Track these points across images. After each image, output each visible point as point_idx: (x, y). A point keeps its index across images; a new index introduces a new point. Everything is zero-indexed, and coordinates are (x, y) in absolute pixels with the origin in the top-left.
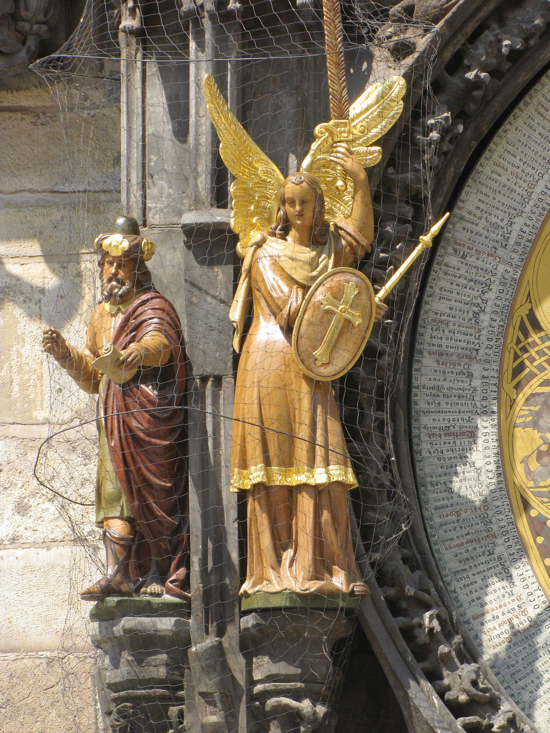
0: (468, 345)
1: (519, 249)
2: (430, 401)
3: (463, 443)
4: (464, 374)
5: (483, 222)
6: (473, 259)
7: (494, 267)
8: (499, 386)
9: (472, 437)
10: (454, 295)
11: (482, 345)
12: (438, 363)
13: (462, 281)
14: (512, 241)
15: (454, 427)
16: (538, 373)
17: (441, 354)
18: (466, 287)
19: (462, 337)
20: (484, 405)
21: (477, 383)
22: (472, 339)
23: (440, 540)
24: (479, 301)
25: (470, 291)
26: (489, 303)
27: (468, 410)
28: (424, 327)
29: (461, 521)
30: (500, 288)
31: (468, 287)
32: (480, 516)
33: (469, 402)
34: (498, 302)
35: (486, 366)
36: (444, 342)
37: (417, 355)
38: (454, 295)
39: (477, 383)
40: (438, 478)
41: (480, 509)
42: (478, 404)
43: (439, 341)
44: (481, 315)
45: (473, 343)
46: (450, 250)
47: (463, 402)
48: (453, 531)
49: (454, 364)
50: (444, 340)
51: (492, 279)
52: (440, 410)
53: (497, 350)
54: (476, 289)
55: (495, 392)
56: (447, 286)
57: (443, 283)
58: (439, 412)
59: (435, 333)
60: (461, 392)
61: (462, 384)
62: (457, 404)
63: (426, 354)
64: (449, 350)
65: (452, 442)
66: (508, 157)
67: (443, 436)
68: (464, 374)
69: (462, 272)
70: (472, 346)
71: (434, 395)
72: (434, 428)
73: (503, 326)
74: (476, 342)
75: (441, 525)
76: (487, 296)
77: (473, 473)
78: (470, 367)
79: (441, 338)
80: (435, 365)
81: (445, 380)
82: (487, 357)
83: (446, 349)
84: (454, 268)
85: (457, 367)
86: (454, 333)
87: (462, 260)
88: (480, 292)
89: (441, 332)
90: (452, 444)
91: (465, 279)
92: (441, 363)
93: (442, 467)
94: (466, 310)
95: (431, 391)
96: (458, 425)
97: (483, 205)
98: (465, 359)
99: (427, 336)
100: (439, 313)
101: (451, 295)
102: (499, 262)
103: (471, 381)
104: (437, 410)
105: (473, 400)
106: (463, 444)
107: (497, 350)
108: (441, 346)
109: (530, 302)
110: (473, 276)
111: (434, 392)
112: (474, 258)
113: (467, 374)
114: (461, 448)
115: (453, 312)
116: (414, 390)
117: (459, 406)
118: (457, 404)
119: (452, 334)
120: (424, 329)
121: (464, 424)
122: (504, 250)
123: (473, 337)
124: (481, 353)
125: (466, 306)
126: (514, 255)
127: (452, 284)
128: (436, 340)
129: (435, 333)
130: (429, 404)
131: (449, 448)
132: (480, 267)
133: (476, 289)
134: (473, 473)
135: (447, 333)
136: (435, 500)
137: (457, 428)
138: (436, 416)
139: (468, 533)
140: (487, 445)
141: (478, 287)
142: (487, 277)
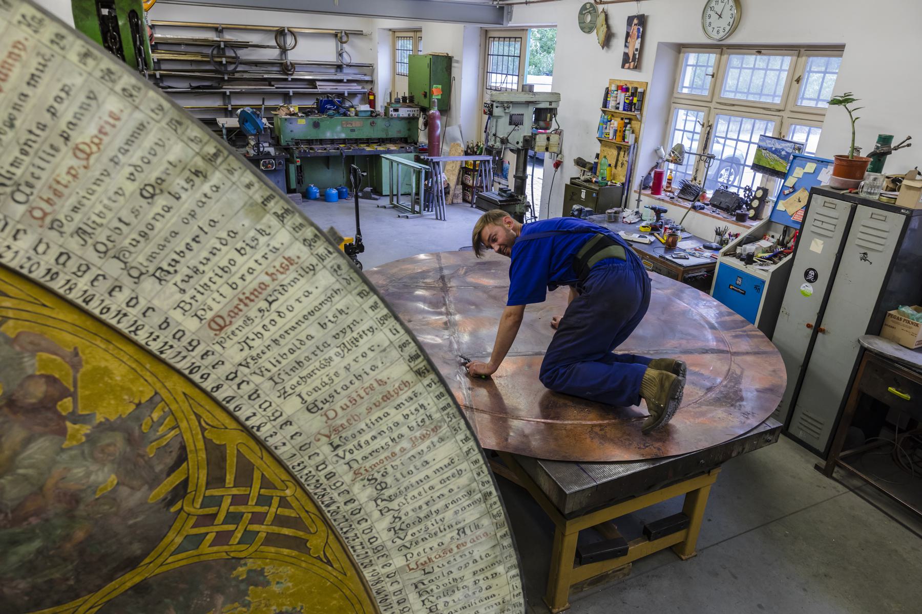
0: (356, 443)
1: (394, 598)
2: (342, 317)
3: (219, 298)
4: (325, 402)
5: (469, 581)
6: (446, 540)
7: (409, 556)
9: (213, 320)
10: (435, 482)
11: (335, 459)
12: (381, 383)
13: (440, 505)
15: (260, 310)
16: (208, 493)
17: (387, 397)
18: (427, 504)
19: (375, 445)
20: (244, 386)
22: (358, 455)
23: (58, 59)
24: (394, 505)
25: (417, 505)
26: (376, 514)
27: (264, 357)
28: (444, 409)
29: (59, 142)
30: (379, 541)
31: (424, 507)
32: (29, 185)
33: (274, 370)
34: (364, 525)
35: (299, 440)
36: (396, 416)
37: (421, 365)
38: (435, 482)
39: (291, 406)
40: (198, 195)
41: (48, 201)
42: (257, 379)
43: (406, 412)
44: (375, 492)
45: (351, 452)
47: (284, 362)
48: (51, 101)
49: (353, 401)
50: (400, 418)
51: (399, 542)
52: (312, 318)
53: (306, 471)
54: (411, 513)
55: (247, 419)
56: (454, 484)
58: (311, 313)
59: (422, 414)
60: (304, 373)
61: (314, 385)
62: (292, 351)
63: (410, 377)
64: (380, 414)
65: (240, 282)
67: (266, 279)
68: (325, 402)
69: (449, 515)
70: (350, 446)
71: (343, 332)
72: (295, 280)
73: (328, 506)
74: (348, 457)
75: (92, 96)
76: (388, 518)
77: (141, 259)
78: (324, 418)
79: (406, 417)
80: (383, 376)
81: (347, 368)
82: (311, 451)
83: (386, 410)
84: (464, 509)
85: (346, 401)
86: (393, 440)
87: (459, 526)
88: (402, 514)
89: (414, 424)
90: (236, 279)
91: (437, 512)
92: (375, 385)
93: (213, 223)
94: (402, 480)
95: (355, 335)
96: (257, 321)
97: (485, 596)
98: (344, 421)
99: (430, 401)
100: (438, 445)
101: (440, 478)
102: (408, 565)
103: (304, 401)
104: (317, 314)
105: (271, 379)
106: (216, 295)
107: (306, 471)
108: (398, 407)
109: (319, 558)
110: (429, 524)
111: (349, 336)
112: (446, 540)
113: (320, 405)
114: (213, 287)
115: (418, 463)
116: (385, 311)
117: (285, 350)
118: (292, 351)
119: (395, 435)
120: (441, 406)
121: (247, 331)
122: (415, 581)
123: (359, 458)
124: (327, 449)
125: (406, 484)
126: (396, 587)
127: (451, 491)
128: (413, 409)
129: (422, 414)
130: (341, 312)
131: (233, 269)
132: (430, 539)
133: (411, 513)
134: (141, 259)
135: (404, 430)
136: (160, 144)
137: (253, 313)
138: (309, 304)
139: (12, 126)
140: (172, 330)
142: (409, 538)
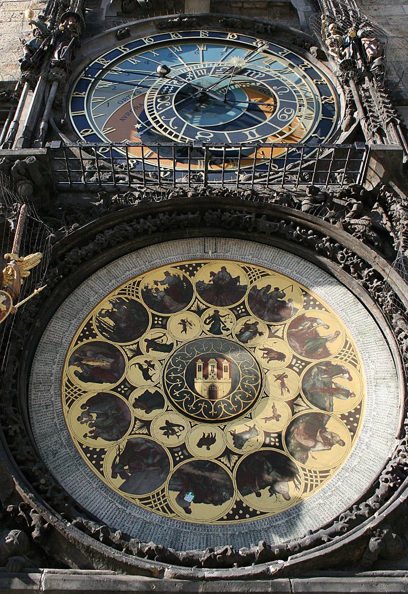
8: (115, 289)
14: (152, 263)
21: (110, 284)
35: (117, 282)
39: (110, 284)
46: (136, 254)
57: (127, 259)
66: (170, 246)
141: (134, 266)
